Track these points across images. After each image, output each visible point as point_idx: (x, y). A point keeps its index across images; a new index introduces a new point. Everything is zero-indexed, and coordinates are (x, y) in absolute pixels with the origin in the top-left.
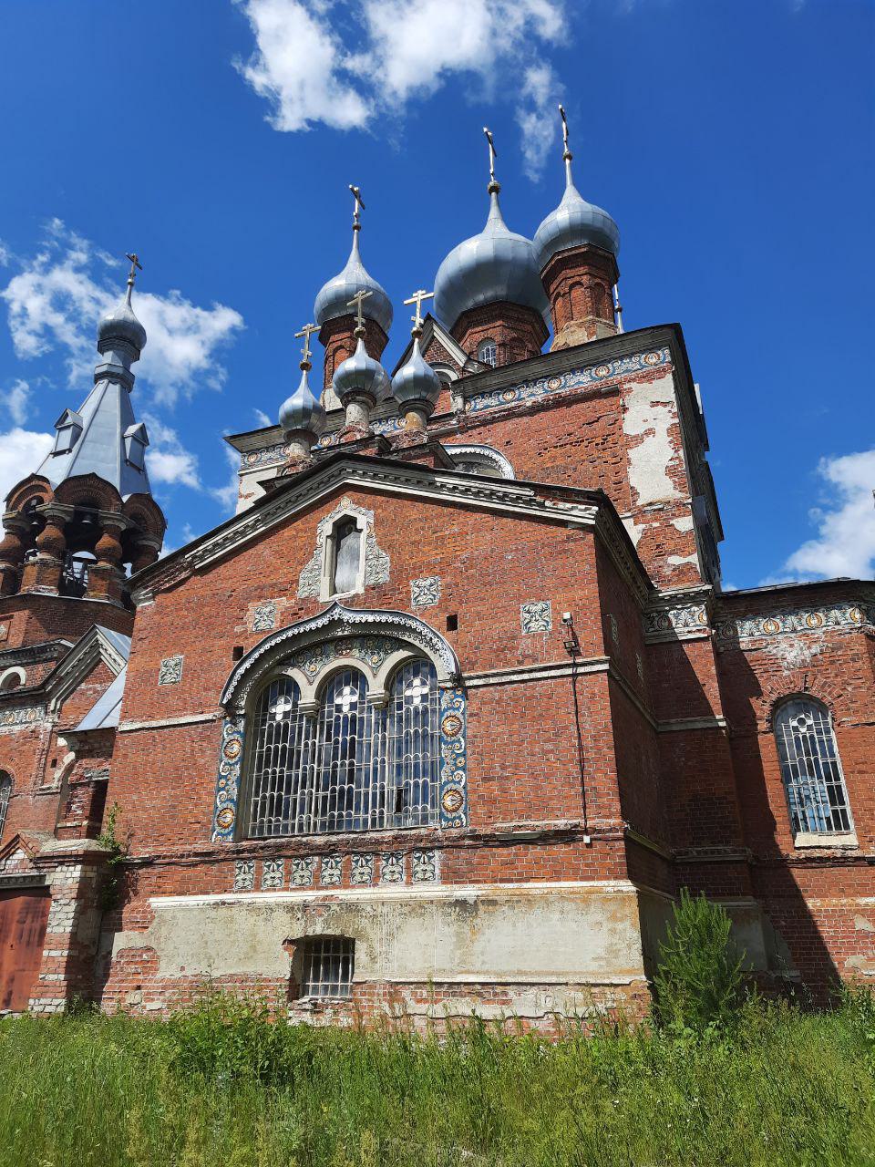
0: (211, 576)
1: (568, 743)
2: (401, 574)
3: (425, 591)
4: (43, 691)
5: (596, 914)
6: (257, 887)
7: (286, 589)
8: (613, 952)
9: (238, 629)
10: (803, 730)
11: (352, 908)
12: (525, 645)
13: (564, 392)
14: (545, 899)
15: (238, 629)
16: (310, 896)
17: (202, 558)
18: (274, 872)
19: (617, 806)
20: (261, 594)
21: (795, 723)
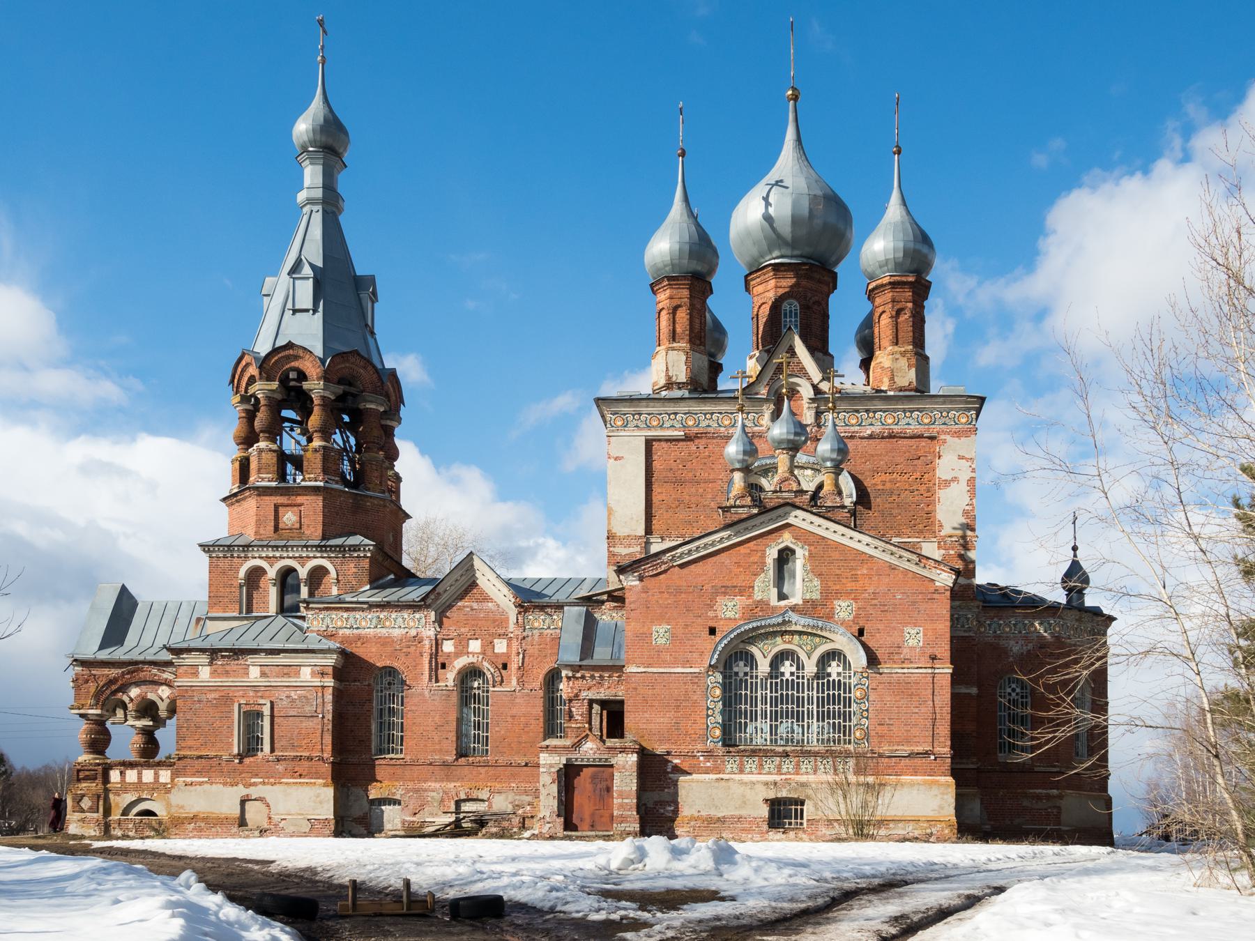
0: (686, 571)
1: (926, 710)
2: (829, 595)
3: (844, 609)
5: (935, 791)
6: (741, 771)
7: (746, 590)
8: (941, 807)
9: (711, 614)
10: (1014, 694)
11: (803, 785)
12: (905, 652)
13: (896, 428)
14: (912, 784)
15: (711, 614)
16: (777, 778)
17: (681, 557)
18: (751, 764)
19: (949, 743)
20: (727, 590)
21: (1009, 690)
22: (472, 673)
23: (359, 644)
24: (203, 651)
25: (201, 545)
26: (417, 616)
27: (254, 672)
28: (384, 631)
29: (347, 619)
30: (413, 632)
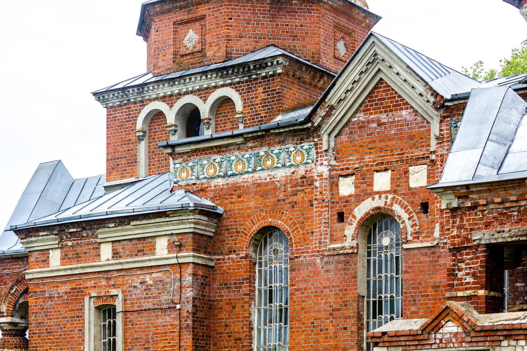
4: (310, 125)
22: (378, 221)
23: (235, 198)
24: (49, 228)
25: (95, 94)
26: (306, 145)
27: (106, 251)
28: (264, 175)
29: (220, 164)
30: (301, 171)
